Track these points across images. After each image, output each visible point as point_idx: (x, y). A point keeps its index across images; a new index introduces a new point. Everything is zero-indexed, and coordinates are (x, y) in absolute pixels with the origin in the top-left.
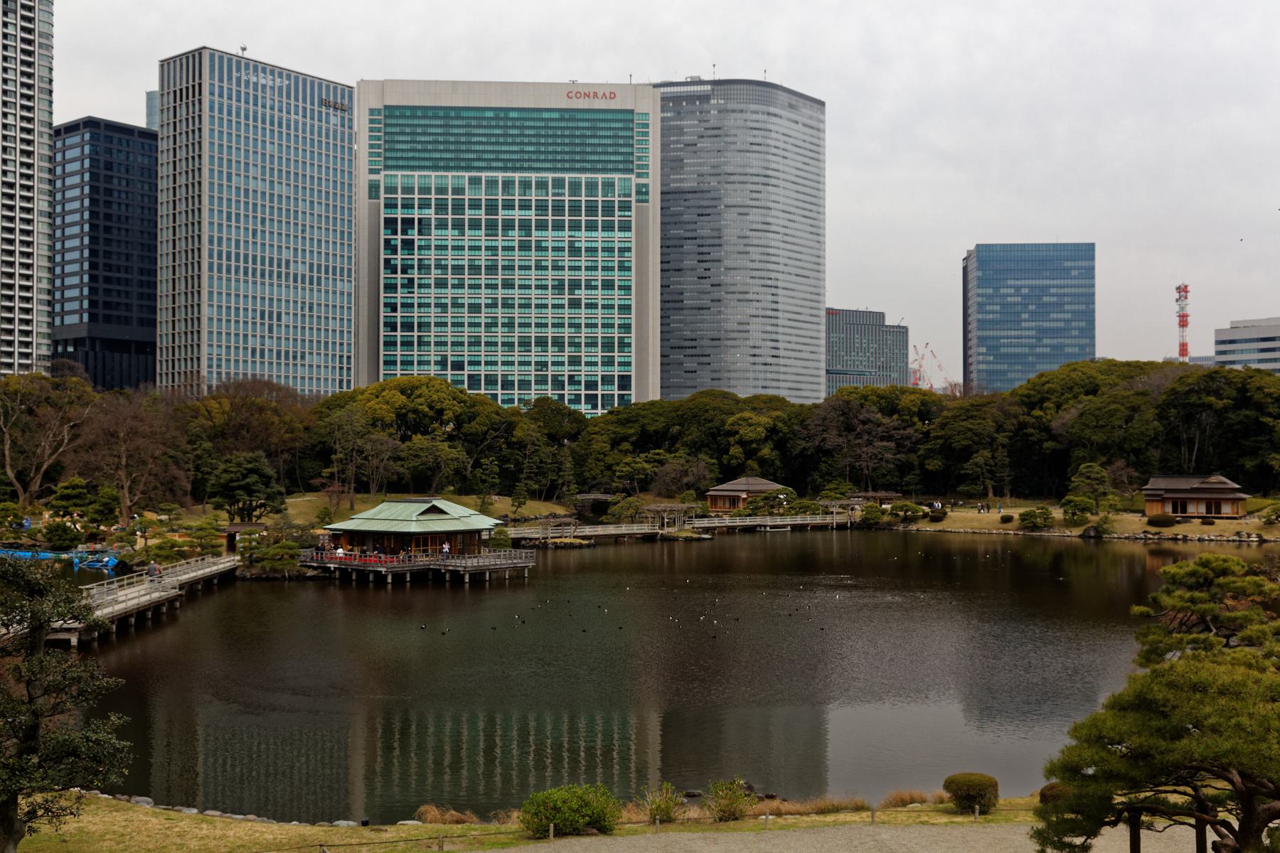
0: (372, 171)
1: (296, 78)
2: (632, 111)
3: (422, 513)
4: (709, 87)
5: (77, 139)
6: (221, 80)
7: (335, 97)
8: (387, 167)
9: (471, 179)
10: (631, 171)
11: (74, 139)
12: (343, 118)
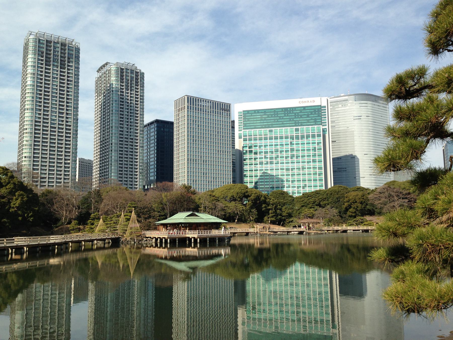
0: (239, 131)
1: (213, 102)
3: (188, 216)
4: (347, 97)
5: (153, 126)
6: (191, 105)
7: (225, 107)
8: (244, 129)
11: (153, 126)
12: (227, 113)
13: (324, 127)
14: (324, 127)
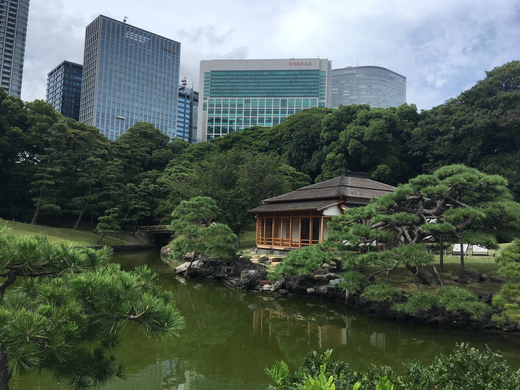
2: (318, 70)
9: (245, 100)
10: (317, 96)
13: (322, 101)
14: (322, 101)
